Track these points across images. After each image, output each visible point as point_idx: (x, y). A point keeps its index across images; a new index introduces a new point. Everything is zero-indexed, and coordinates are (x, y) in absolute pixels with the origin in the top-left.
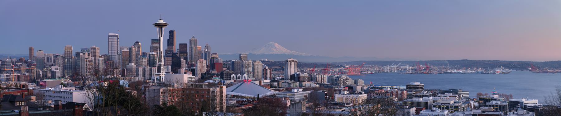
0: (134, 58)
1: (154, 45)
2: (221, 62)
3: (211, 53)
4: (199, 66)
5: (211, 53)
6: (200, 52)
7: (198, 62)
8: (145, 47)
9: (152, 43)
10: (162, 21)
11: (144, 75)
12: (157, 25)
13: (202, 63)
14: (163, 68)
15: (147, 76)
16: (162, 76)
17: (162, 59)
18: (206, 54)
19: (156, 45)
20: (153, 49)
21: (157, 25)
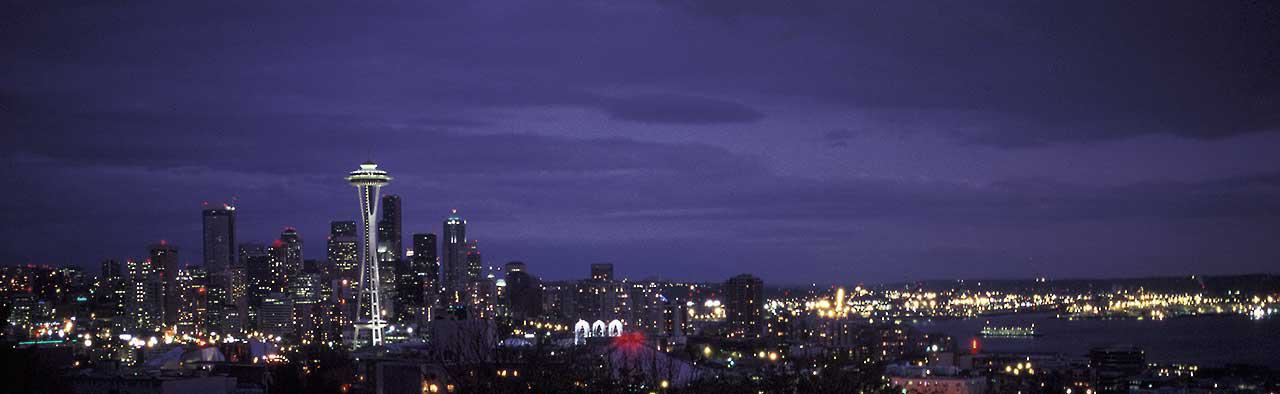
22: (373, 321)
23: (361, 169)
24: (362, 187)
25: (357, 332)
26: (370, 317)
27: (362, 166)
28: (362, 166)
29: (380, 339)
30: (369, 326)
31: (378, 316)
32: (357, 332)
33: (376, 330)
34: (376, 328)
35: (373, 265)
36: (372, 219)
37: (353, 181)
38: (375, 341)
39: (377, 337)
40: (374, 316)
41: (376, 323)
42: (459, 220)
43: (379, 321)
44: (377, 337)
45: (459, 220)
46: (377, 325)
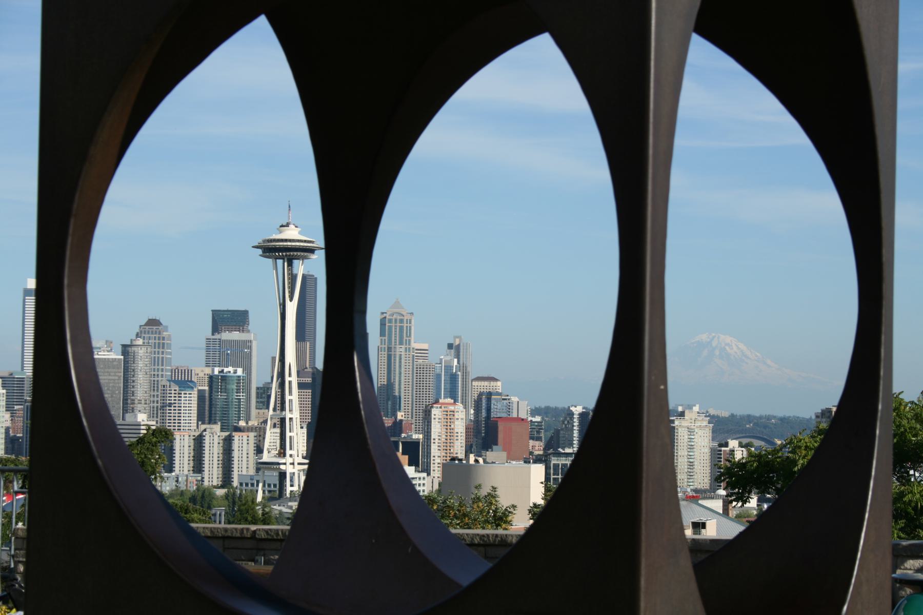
0: (141, 388)
1: (226, 336)
2: (523, 415)
3: (472, 375)
4: (436, 429)
5: (473, 373)
6: (420, 372)
7: (436, 412)
8: (189, 347)
9: (216, 329)
10: (292, 233)
11: (198, 466)
12: (271, 250)
13: (449, 417)
15: (212, 475)
16: (289, 469)
17: (294, 397)
18: (453, 378)
19: (235, 336)
20: (218, 353)
21: (271, 250)
22: (289, 460)
26: (282, 454)
30: (282, 467)
34: (293, 471)
35: (290, 375)
38: (289, 489)
40: (288, 452)
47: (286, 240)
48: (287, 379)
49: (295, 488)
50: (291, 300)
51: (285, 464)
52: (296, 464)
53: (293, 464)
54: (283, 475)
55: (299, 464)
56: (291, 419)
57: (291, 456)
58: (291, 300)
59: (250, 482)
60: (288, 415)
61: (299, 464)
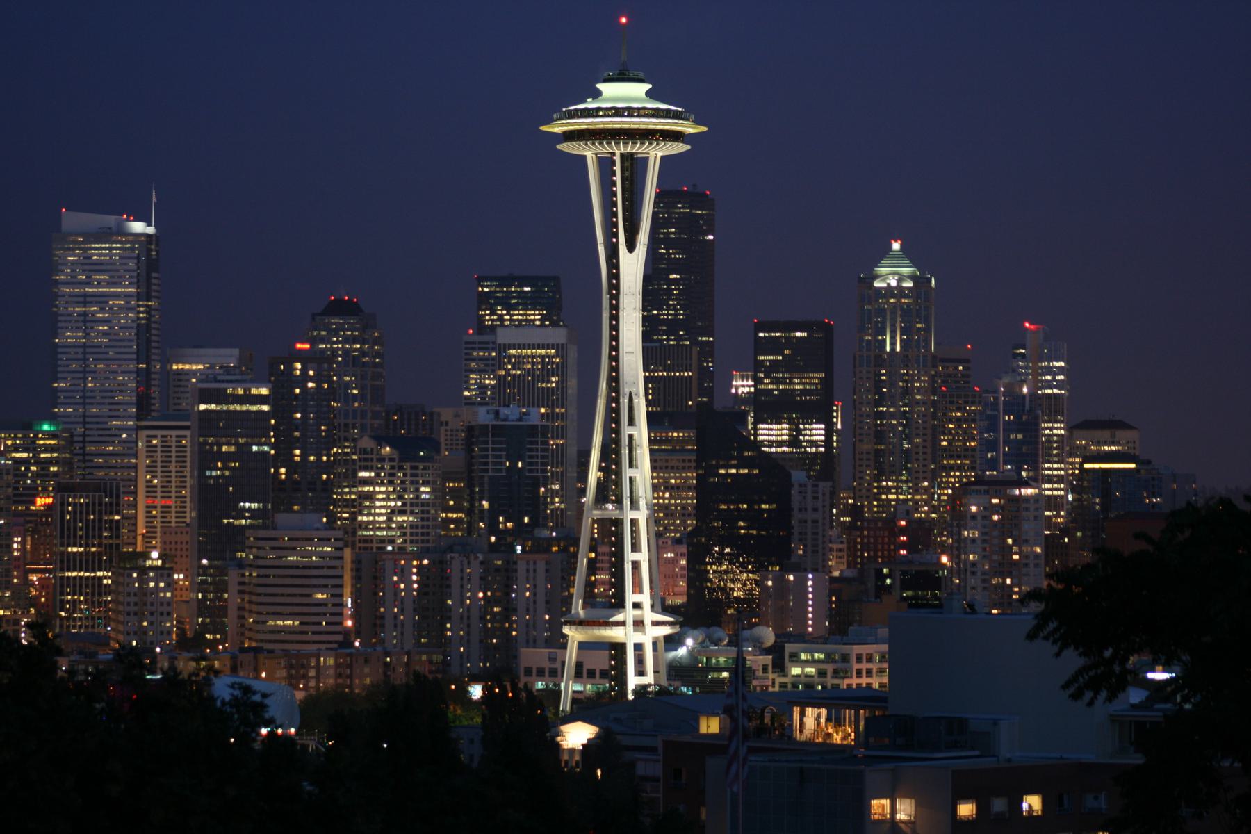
14: (639, 557)
22: (629, 614)
23: (597, 94)
24: (605, 165)
25: (572, 655)
26: (620, 604)
27: (599, 86)
28: (599, 86)
29: (649, 679)
31: (645, 598)
32: (572, 655)
33: (639, 647)
35: (631, 422)
36: (632, 266)
37: (570, 136)
38: (633, 681)
39: (641, 673)
40: (631, 598)
41: (639, 624)
42: (912, 277)
43: (649, 616)
44: (641, 673)
45: (912, 277)
46: (641, 629)
47: (618, 112)
48: (627, 430)
49: (649, 679)
50: (631, 247)
51: (623, 624)
52: (647, 622)
53: (639, 624)
54: (619, 648)
55: (655, 623)
56: (634, 522)
57: (637, 606)
58: (631, 247)
59: (547, 665)
60: (629, 515)
61: (655, 623)
